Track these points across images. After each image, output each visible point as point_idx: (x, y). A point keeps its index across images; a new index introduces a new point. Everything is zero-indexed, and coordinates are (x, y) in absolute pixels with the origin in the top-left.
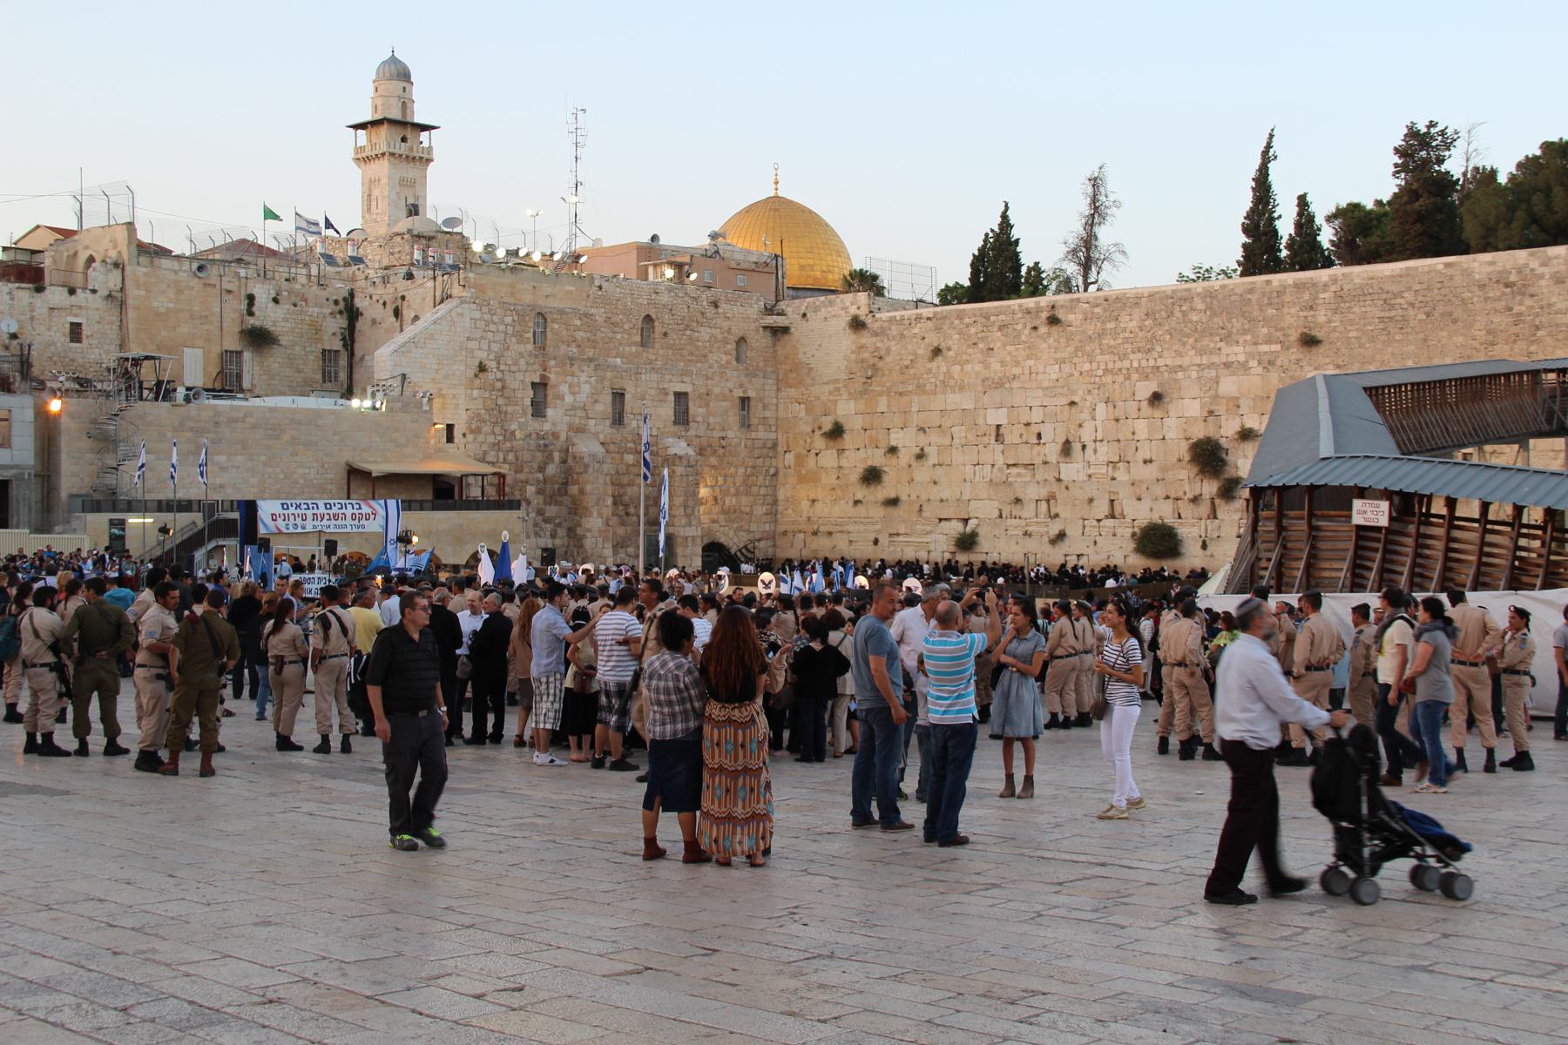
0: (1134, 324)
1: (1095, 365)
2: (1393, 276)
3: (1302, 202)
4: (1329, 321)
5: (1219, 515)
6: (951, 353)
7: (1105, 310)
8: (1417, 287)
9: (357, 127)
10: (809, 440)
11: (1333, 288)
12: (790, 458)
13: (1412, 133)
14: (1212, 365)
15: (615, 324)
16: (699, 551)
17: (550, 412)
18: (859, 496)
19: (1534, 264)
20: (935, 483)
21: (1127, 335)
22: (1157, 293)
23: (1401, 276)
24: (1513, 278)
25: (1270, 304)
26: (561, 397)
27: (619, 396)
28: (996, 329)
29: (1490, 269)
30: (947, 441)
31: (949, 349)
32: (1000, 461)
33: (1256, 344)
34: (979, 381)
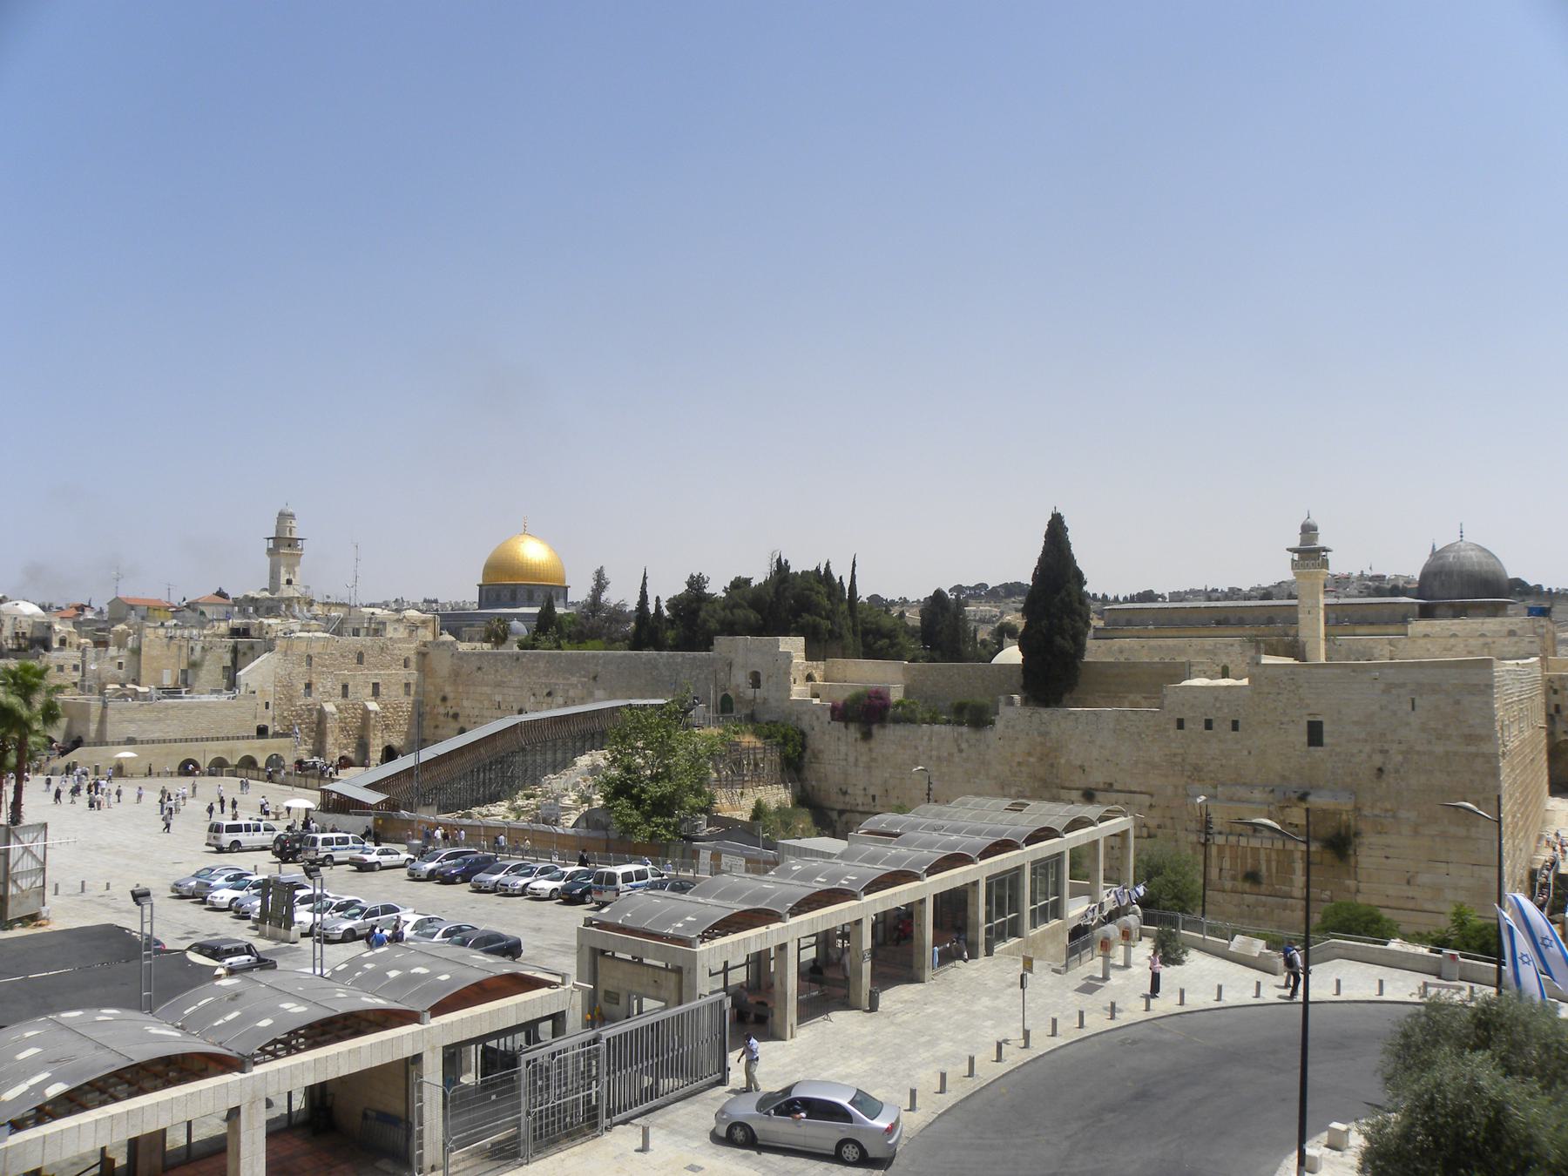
0: (543, 666)
3: (658, 598)
9: (268, 539)
12: (428, 708)
13: (692, 577)
15: (345, 656)
16: (381, 749)
17: (313, 695)
19: (658, 657)
26: (318, 689)
27: (345, 687)
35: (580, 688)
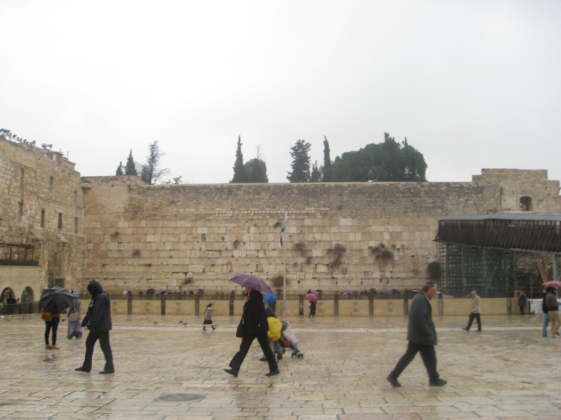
0: (267, 197)
1: (249, 212)
2: (370, 187)
4: (348, 201)
5: (304, 270)
6: (179, 204)
7: (254, 190)
8: (380, 191)
10: (102, 238)
11: (349, 189)
14: (301, 214)
18: (130, 262)
19: (419, 187)
20: (171, 257)
21: (264, 201)
22: (277, 185)
23: (374, 187)
24: (412, 191)
25: (325, 193)
27: (43, 212)
28: (202, 195)
29: (405, 187)
30: (177, 240)
31: (178, 202)
32: (204, 248)
33: (319, 207)
34: (194, 216)
35: (321, 217)
